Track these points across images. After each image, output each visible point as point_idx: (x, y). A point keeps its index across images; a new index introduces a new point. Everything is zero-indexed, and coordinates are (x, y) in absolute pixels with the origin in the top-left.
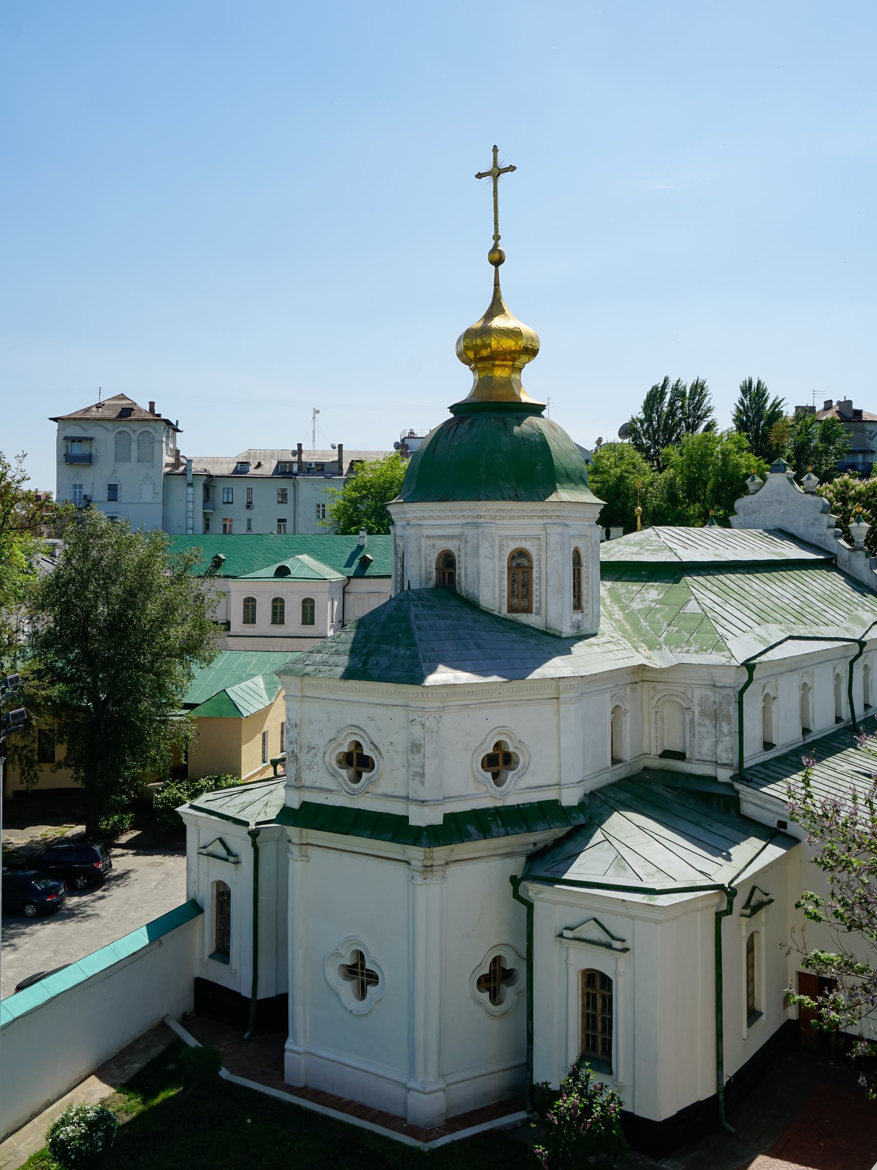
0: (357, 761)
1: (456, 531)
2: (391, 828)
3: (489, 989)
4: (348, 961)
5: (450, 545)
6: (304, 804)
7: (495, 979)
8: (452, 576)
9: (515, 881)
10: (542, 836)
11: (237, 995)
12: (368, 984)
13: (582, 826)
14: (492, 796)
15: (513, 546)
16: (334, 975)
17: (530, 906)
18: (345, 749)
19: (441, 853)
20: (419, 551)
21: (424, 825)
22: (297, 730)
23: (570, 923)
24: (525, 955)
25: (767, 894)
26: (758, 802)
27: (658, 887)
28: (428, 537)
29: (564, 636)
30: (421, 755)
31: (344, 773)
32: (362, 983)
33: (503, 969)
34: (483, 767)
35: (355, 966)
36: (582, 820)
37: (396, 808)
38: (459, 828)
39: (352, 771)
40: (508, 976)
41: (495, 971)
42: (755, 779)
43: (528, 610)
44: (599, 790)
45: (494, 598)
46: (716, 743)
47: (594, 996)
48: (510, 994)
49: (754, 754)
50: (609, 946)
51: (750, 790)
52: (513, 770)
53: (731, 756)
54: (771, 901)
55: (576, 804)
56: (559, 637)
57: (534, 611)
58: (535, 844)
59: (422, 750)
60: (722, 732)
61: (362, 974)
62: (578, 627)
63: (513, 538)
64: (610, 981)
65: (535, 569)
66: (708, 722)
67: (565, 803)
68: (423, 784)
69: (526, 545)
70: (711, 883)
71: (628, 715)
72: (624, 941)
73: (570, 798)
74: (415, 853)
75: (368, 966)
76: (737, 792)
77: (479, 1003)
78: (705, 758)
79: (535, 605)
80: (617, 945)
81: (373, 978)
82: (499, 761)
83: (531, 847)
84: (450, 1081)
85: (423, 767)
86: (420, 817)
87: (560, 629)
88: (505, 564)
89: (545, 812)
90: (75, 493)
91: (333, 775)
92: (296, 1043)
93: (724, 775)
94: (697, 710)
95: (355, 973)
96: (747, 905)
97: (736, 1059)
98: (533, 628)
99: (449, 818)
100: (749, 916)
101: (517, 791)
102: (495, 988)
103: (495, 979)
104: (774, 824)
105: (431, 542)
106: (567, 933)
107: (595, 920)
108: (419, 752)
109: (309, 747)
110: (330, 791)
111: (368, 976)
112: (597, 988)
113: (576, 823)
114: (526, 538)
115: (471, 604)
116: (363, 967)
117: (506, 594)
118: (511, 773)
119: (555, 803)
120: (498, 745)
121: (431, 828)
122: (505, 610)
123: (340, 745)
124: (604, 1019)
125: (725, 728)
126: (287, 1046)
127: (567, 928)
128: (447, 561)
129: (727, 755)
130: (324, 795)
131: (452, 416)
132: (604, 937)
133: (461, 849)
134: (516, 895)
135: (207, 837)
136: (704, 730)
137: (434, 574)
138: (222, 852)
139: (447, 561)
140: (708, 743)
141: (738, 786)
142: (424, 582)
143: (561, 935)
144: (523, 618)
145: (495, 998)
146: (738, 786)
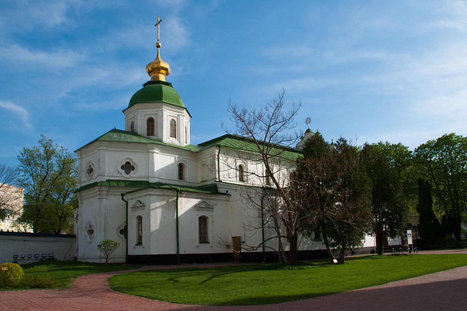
15: (149, 116)
16: (86, 234)
17: (127, 203)
43: (153, 135)
45: (142, 131)
63: (148, 114)
67: (150, 182)
69: (152, 116)
71: (188, 168)
82: (128, 167)
88: (146, 122)
101: (133, 176)
114: (152, 114)
117: (146, 131)
134: (123, 199)
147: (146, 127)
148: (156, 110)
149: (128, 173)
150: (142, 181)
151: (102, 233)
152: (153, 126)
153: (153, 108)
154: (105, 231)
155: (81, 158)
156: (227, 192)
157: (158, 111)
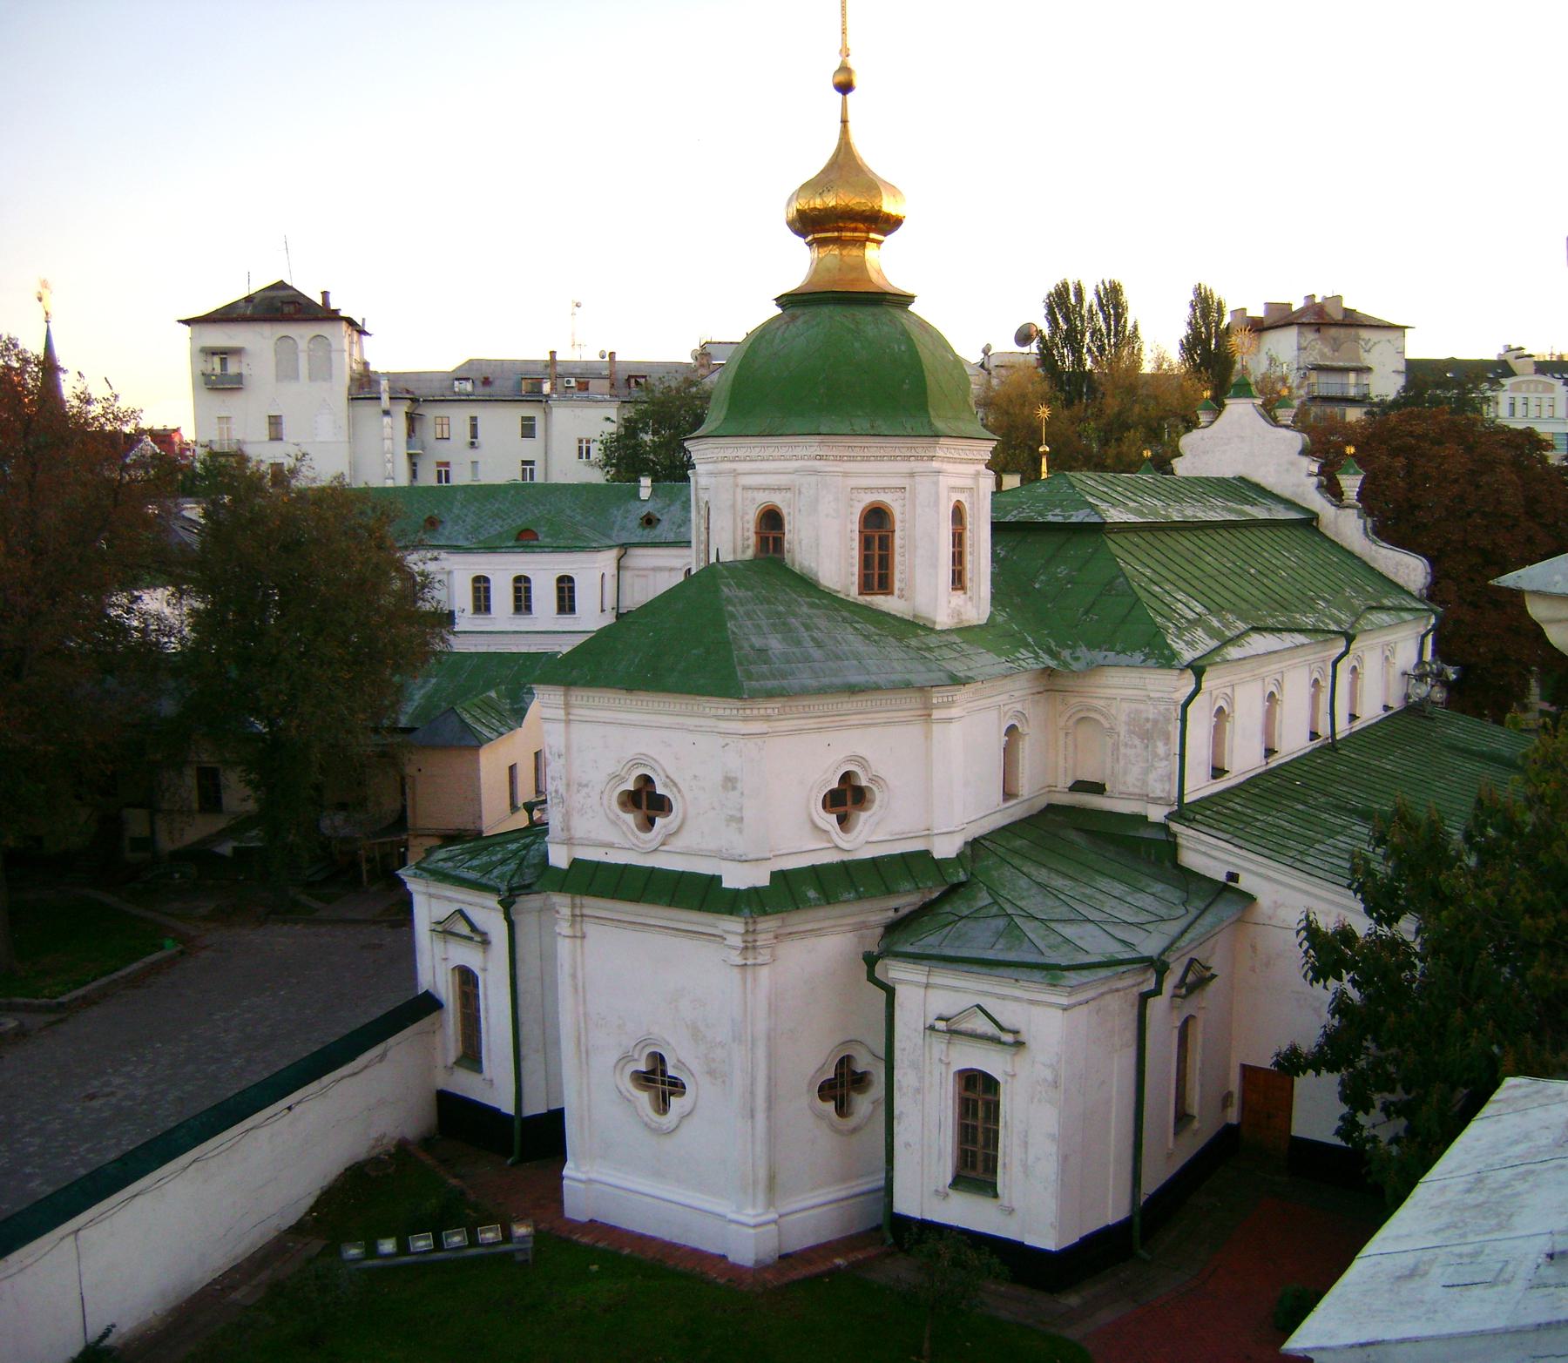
0: (646, 801)
1: (783, 480)
2: (697, 893)
3: (835, 1099)
4: (642, 1066)
5: (777, 500)
6: (575, 863)
7: (842, 1085)
8: (778, 543)
9: (870, 960)
10: (907, 901)
11: (496, 1111)
12: (671, 1094)
13: (961, 884)
14: (837, 847)
15: (868, 499)
16: (628, 1085)
17: (890, 992)
18: (630, 786)
19: (767, 924)
20: (734, 506)
21: (742, 886)
22: (562, 761)
23: (946, 1013)
24: (882, 1053)
25: (1208, 969)
26: (1203, 849)
27: (1064, 962)
28: (745, 488)
29: (938, 627)
30: (737, 793)
31: (630, 818)
32: (664, 1093)
33: (854, 1073)
34: (824, 807)
35: (653, 1072)
36: (962, 877)
37: (705, 867)
38: (791, 892)
39: (640, 814)
40: (860, 1081)
41: (842, 1075)
42: (1198, 817)
44: (983, 837)
46: (1146, 772)
47: (975, 1102)
48: (865, 1104)
49: (1199, 786)
50: (998, 1041)
51: (1191, 832)
52: (864, 810)
53: (1167, 787)
54: (1214, 976)
55: (953, 855)
56: (932, 630)
57: (896, 592)
58: (896, 910)
59: (739, 785)
60: (1155, 755)
61: (663, 1083)
62: (959, 614)
64: (997, 1083)
65: (897, 534)
66: (1137, 742)
67: (937, 856)
68: (740, 831)
69: (886, 498)
70: (1134, 955)
72: (1016, 1032)
73: (945, 849)
74: (732, 927)
75: (671, 1072)
76: (1175, 836)
77: (820, 1116)
78: (1131, 790)
79: (897, 585)
80: (1008, 1038)
81: (677, 1087)
82: (847, 798)
83: (891, 914)
84: (783, 1210)
85: (741, 809)
86: (736, 878)
87: (931, 616)
88: (856, 527)
89: (915, 864)
90: (221, 429)
91: (613, 823)
92: (577, 1168)
93: (1157, 814)
94: (1123, 730)
95: (654, 1081)
96: (1182, 982)
97: (1155, 1177)
98: (894, 617)
99: (779, 877)
100: (1184, 997)
101: (871, 837)
102: (842, 1096)
103: (840, 1085)
104: (1222, 878)
105: (750, 494)
106: (941, 1025)
107: (978, 1006)
108: (734, 788)
109: (580, 785)
110: (611, 846)
111: (671, 1084)
112: (978, 1092)
113: (955, 881)
115: (807, 584)
116: (664, 1073)
117: (856, 570)
118: (863, 816)
119: (926, 854)
120: (847, 777)
121: (754, 891)
122: (854, 591)
123: (623, 780)
124: (987, 1130)
125: (1161, 749)
126: (566, 1172)
127: (940, 1018)
128: (771, 520)
129: (1161, 786)
130: (604, 850)
131: (779, 311)
132: (990, 1029)
133: (799, 921)
134: (872, 978)
135: (443, 910)
136: (1130, 752)
137: (753, 540)
138: (464, 929)
139: (771, 520)
140: (1135, 771)
141: (1175, 827)
142: (739, 550)
143: (932, 1028)
144: (881, 602)
145: (843, 1109)
146: (1175, 827)
147: (856, 553)
148: (904, 466)
149: (843, 821)
150: (905, 858)
151: (761, 1116)
152: (886, 543)
153: (893, 458)
154: (769, 1108)
155: (568, 722)
156: (1233, 877)
157: (912, 475)
